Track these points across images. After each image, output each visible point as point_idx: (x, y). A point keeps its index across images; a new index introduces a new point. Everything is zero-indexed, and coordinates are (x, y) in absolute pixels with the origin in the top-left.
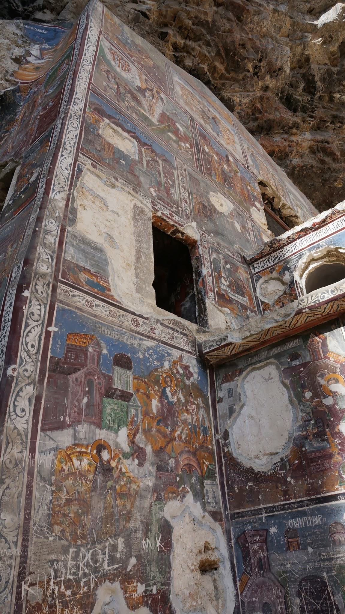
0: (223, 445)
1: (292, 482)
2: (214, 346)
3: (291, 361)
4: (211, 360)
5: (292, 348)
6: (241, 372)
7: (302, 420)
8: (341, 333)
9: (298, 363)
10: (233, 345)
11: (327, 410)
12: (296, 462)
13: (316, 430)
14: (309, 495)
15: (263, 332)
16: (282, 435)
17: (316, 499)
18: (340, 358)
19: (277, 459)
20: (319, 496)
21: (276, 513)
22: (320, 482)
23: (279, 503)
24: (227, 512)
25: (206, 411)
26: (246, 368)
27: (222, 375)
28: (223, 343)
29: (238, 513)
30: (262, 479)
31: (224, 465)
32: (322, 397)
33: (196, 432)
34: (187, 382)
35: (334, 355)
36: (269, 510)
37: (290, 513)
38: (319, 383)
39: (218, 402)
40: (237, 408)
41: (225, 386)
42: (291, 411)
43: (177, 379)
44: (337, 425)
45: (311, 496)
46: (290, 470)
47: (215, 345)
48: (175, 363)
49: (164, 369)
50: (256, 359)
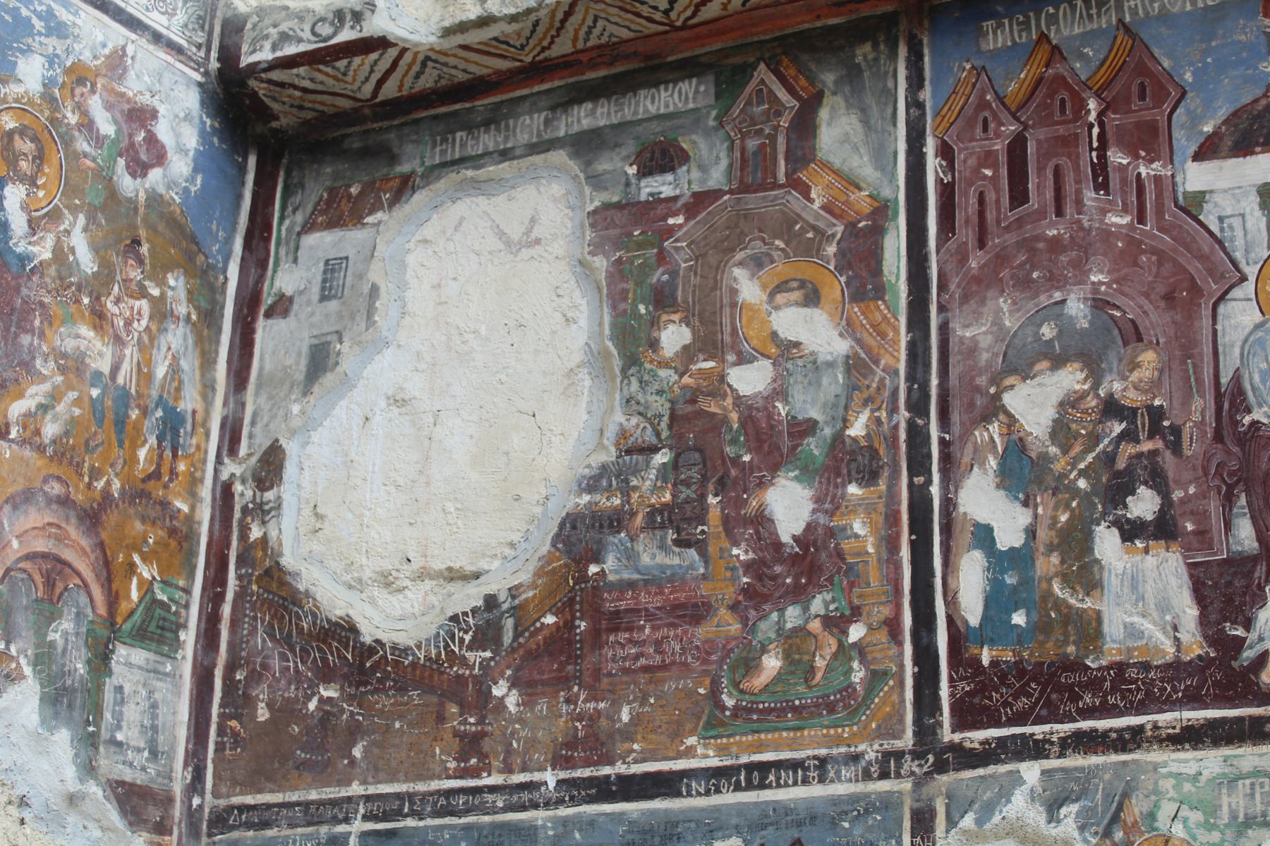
0: (245, 510)
1: (512, 702)
2: (300, 40)
3: (644, 172)
4: (275, 106)
5: (659, 117)
6: (405, 187)
7: (617, 444)
8: (890, 84)
9: (667, 192)
10: (392, 53)
11: (734, 416)
12: (550, 619)
13: (667, 497)
14: (568, 763)
15: (543, 13)
16: (518, 498)
17: (591, 781)
18: (854, 196)
19: (468, 597)
20: (607, 770)
21: (410, 822)
22: (625, 716)
23: (435, 785)
24: (196, 801)
25: (199, 340)
26: (433, 173)
27: (314, 192)
28: (346, 35)
29: (242, 808)
30: (387, 676)
31: (230, 596)
32: (731, 358)
33: (120, 422)
34: (127, 184)
35: (830, 178)
36: (384, 808)
37: (468, 828)
38: (734, 292)
39: (268, 315)
40: (347, 351)
41: (321, 243)
42: (585, 398)
43: (73, 156)
44: (762, 484)
45: (574, 767)
46: (513, 650)
47: (307, 34)
48: (79, 76)
49: (15, 89)
50: (488, 141)
